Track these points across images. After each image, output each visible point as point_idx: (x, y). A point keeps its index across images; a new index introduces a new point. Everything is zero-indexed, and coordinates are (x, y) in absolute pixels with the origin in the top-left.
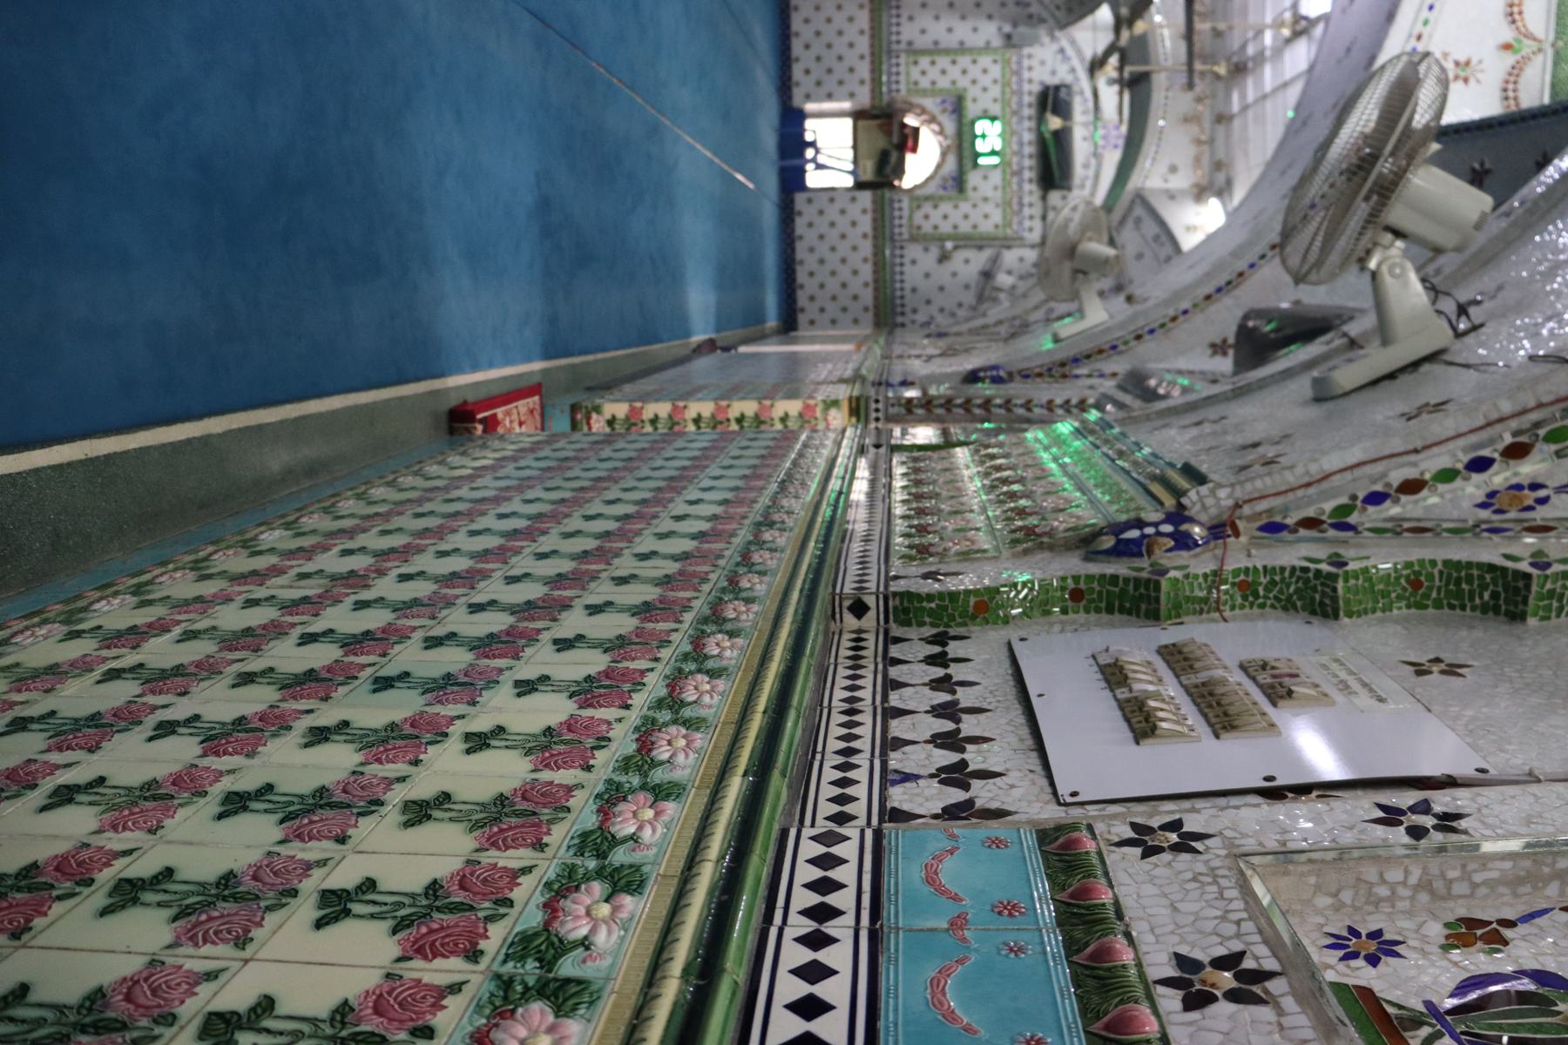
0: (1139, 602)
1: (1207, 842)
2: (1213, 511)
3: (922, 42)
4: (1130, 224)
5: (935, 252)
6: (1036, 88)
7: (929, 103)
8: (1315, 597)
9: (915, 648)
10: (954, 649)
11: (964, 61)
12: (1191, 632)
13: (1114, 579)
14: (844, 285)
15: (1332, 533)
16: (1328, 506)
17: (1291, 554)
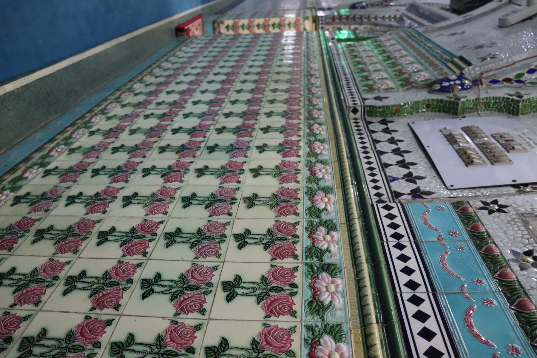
0: (451, 109)
1: (508, 208)
2: (473, 75)
9: (378, 127)
10: (391, 126)
12: (469, 121)
13: (442, 101)
15: (515, 84)
16: (514, 74)
17: (502, 92)
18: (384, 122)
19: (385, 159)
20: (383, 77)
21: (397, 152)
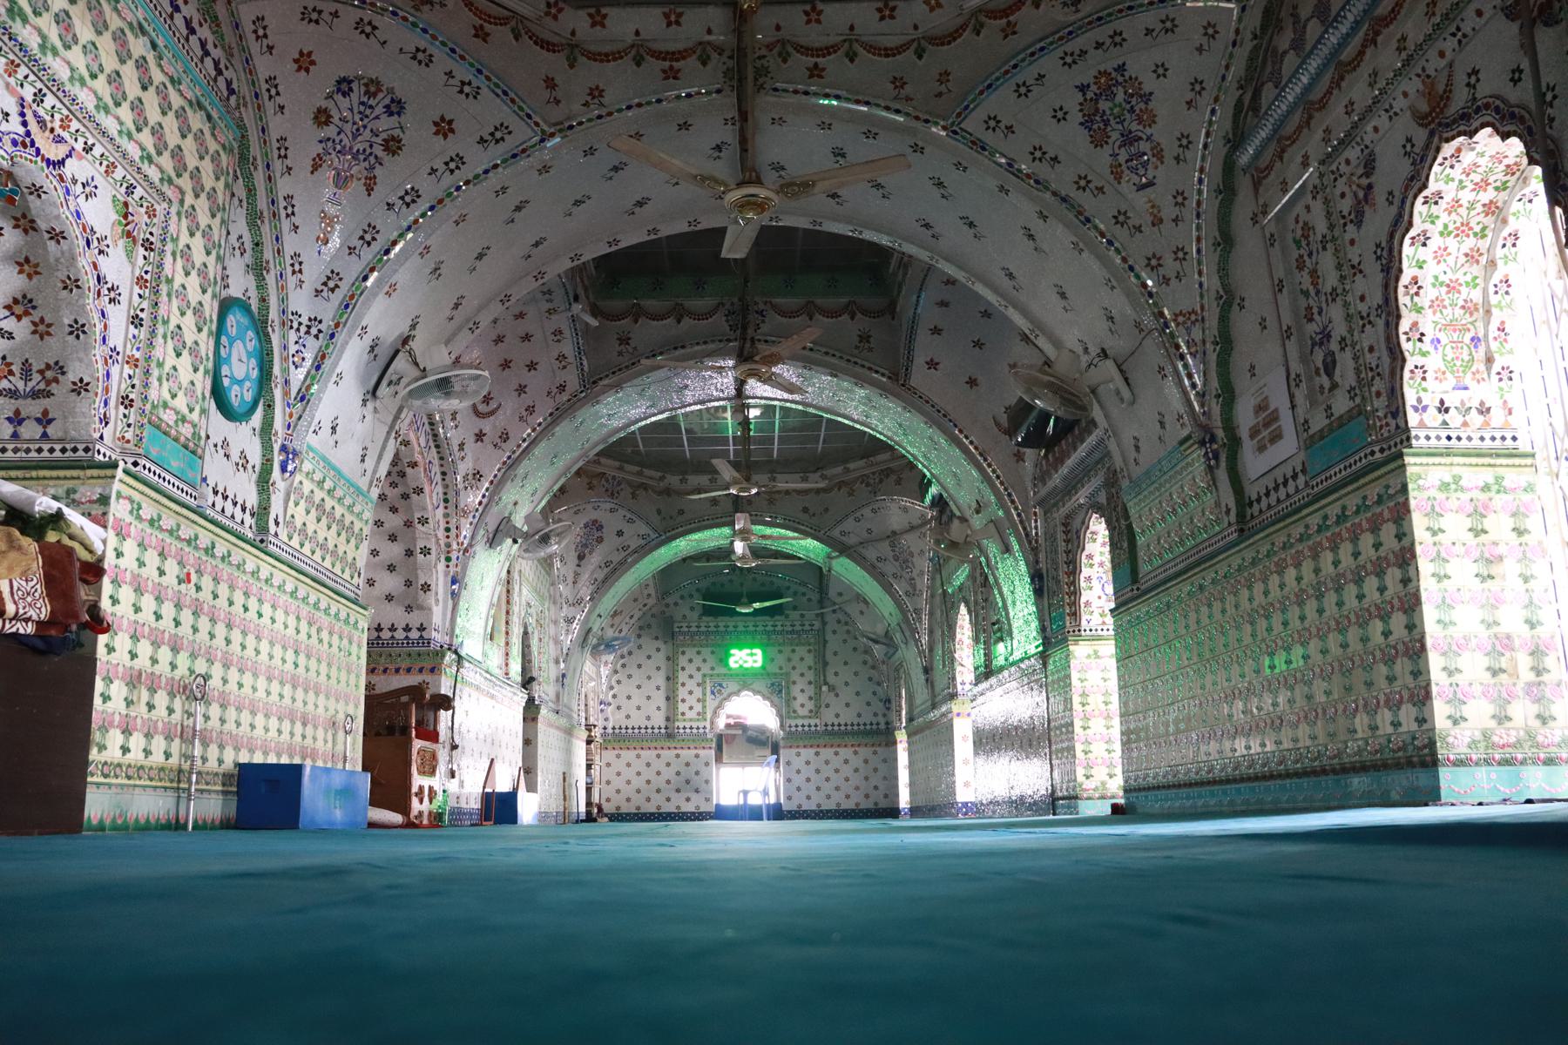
9: (1256, 507)
12: (1244, 433)
18: (1251, 504)
19: (1283, 497)
21: (1276, 488)
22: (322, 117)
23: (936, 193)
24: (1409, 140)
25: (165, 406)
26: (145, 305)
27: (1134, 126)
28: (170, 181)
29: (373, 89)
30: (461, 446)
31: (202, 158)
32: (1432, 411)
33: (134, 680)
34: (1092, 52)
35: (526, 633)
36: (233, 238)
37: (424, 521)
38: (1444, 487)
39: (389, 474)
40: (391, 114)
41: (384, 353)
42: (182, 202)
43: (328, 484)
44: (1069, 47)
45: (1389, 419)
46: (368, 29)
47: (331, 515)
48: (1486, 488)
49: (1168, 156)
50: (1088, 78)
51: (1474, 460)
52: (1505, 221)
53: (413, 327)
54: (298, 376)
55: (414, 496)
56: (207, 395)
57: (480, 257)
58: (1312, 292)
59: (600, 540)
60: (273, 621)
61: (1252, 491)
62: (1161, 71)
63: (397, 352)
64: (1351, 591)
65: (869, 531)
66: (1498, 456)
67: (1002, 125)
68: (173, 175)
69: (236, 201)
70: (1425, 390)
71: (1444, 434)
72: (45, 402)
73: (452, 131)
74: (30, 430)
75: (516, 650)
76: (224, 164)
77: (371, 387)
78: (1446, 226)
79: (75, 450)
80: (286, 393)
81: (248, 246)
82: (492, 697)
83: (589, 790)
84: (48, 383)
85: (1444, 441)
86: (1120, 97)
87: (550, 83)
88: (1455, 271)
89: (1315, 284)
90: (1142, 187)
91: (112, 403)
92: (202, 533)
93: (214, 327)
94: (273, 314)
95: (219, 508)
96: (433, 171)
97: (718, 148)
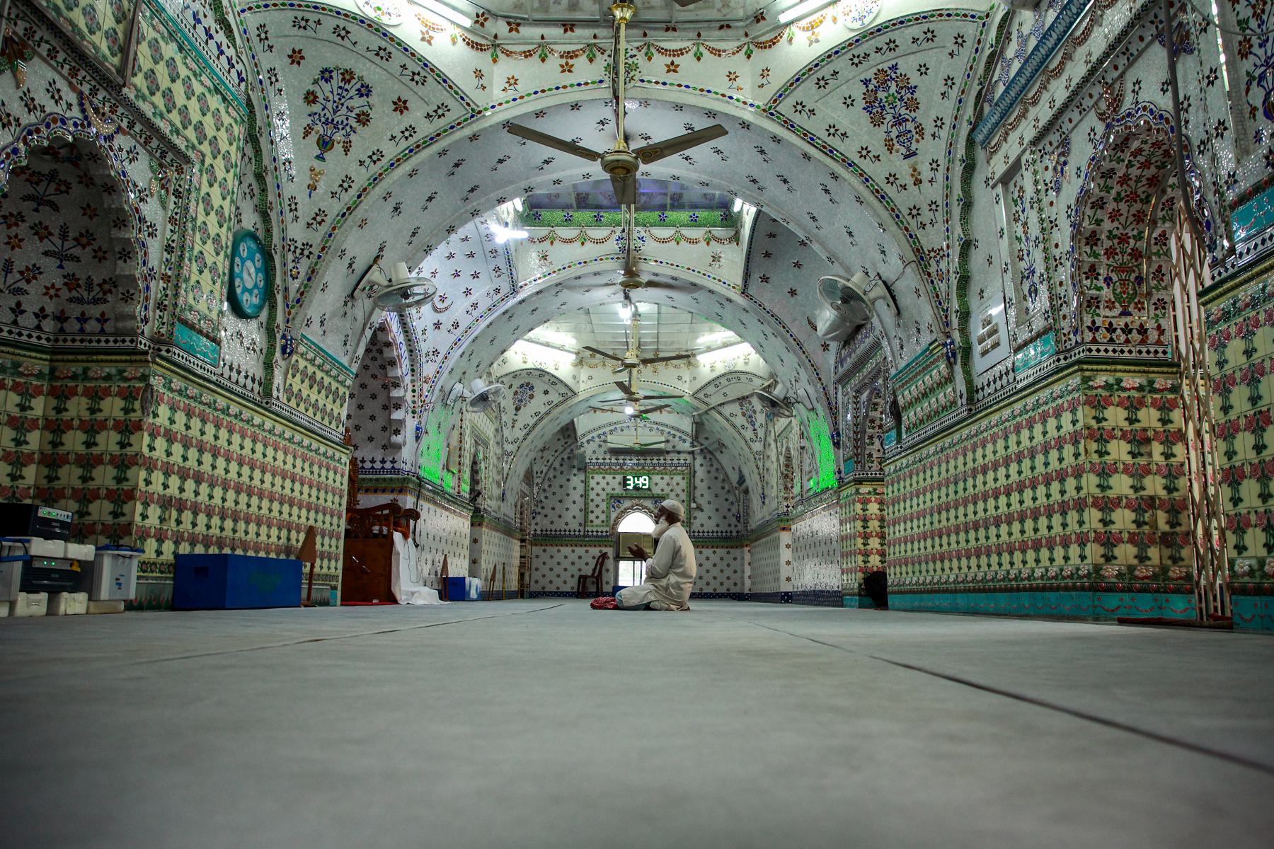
0: (967, 351)
3: (580, 516)
4: (706, 400)
5: (697, 513)
6: (608, 456)
7: (614, 515)
8: (965, 316)
9: (981, 394)
11: (592, 495)
14: (715, 565)
17: (955, 322)
18: (977, 391)
20: (942, 397)
22: (311, 98)
23: (760, 157)
24: (1092, 130)
25: (191, 308)
26: (175, 237)
27: (903, 111)
28: (194, 147)
29: (347, 77)
30: (424, 332)
31: (218, 130)
32: (1103, 331)
33: (166, 503)
34: (873, 55)
35: (474, 463)
36: (245, 185)
37: (396, 385)
38: (1108, 386)
39: (368, 351)
40: (362, 96)
41: (359, 266)
42: (203, 162)
43: (319, 361)
44: (856, 52)
45: (1071, 336)
46: (343, 33)
47: (321, 384)
48: (1141, 388)
49: (927, 136)
50: (869, 74)
51: (1132, 368)
52: (1164, 192)
53: (381, 249)
54: (294, 285)
55: (389, 367)
56: (224, 298)
57: (430, 199)
58: (1024, 239)
59: (532, 397)
60: (275, 459)
61: (979, 382)
62: (923, 70)
63: (370, 267)
64: (1040, 459)
65: (725, 394)
66: (1151, 365)
67: (806, 109)
68: (196, 143)
69: (246, 159)
70: (1098, 315)
71: (1110, 348)
72: (102, 307)
73: (407, 108)
74: (92, 326)
75: (466, 475)
76: (236, 133)
77: (349, 291)
78: (1118, 194)
79: (124, 341)
80: (286, 298)
81: (256, 191)
82: (447, 509)
83: (522, 575)
84: (105, 293)
85: (1111, 353)
86: (893, 89)
87: (479, 74)
88: (1125, 227)
89: (1025, 233)
90: (906, 157)
91: (151, 307)
92: (219, 399)
93: (229, 251)
94: (276, 240)
95: (234, 379)
96: (393, 138)
97: (602, 123)
